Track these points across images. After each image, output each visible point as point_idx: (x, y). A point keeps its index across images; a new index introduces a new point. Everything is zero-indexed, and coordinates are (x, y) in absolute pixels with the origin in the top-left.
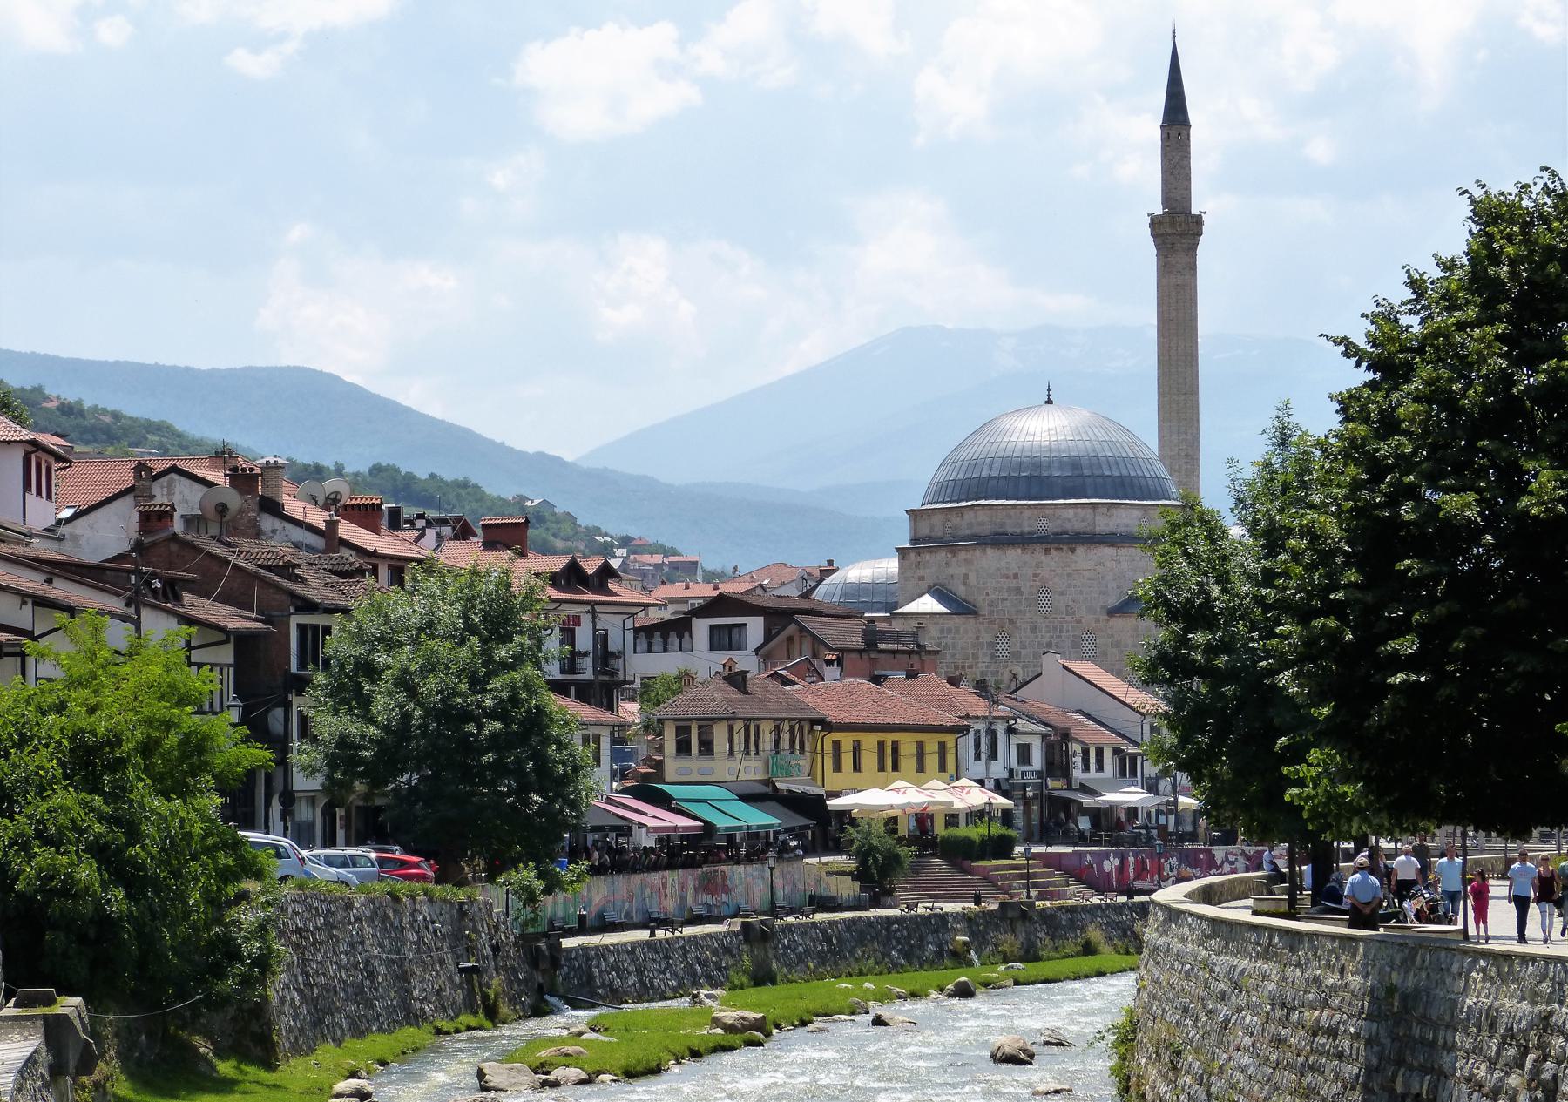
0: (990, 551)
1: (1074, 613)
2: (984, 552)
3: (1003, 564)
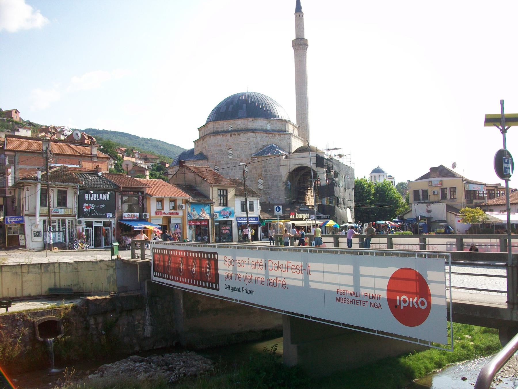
0: (212, 137)
1: (240, 157)
2: (210, 137)
3: (216, 141)
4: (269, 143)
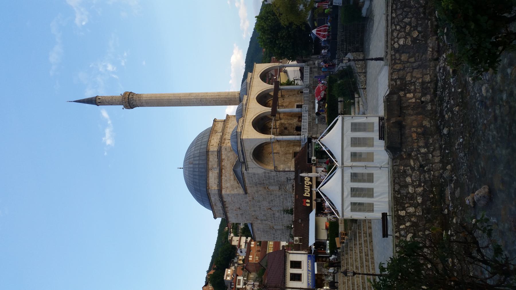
2: (230, 221)
4: (232, 173)
